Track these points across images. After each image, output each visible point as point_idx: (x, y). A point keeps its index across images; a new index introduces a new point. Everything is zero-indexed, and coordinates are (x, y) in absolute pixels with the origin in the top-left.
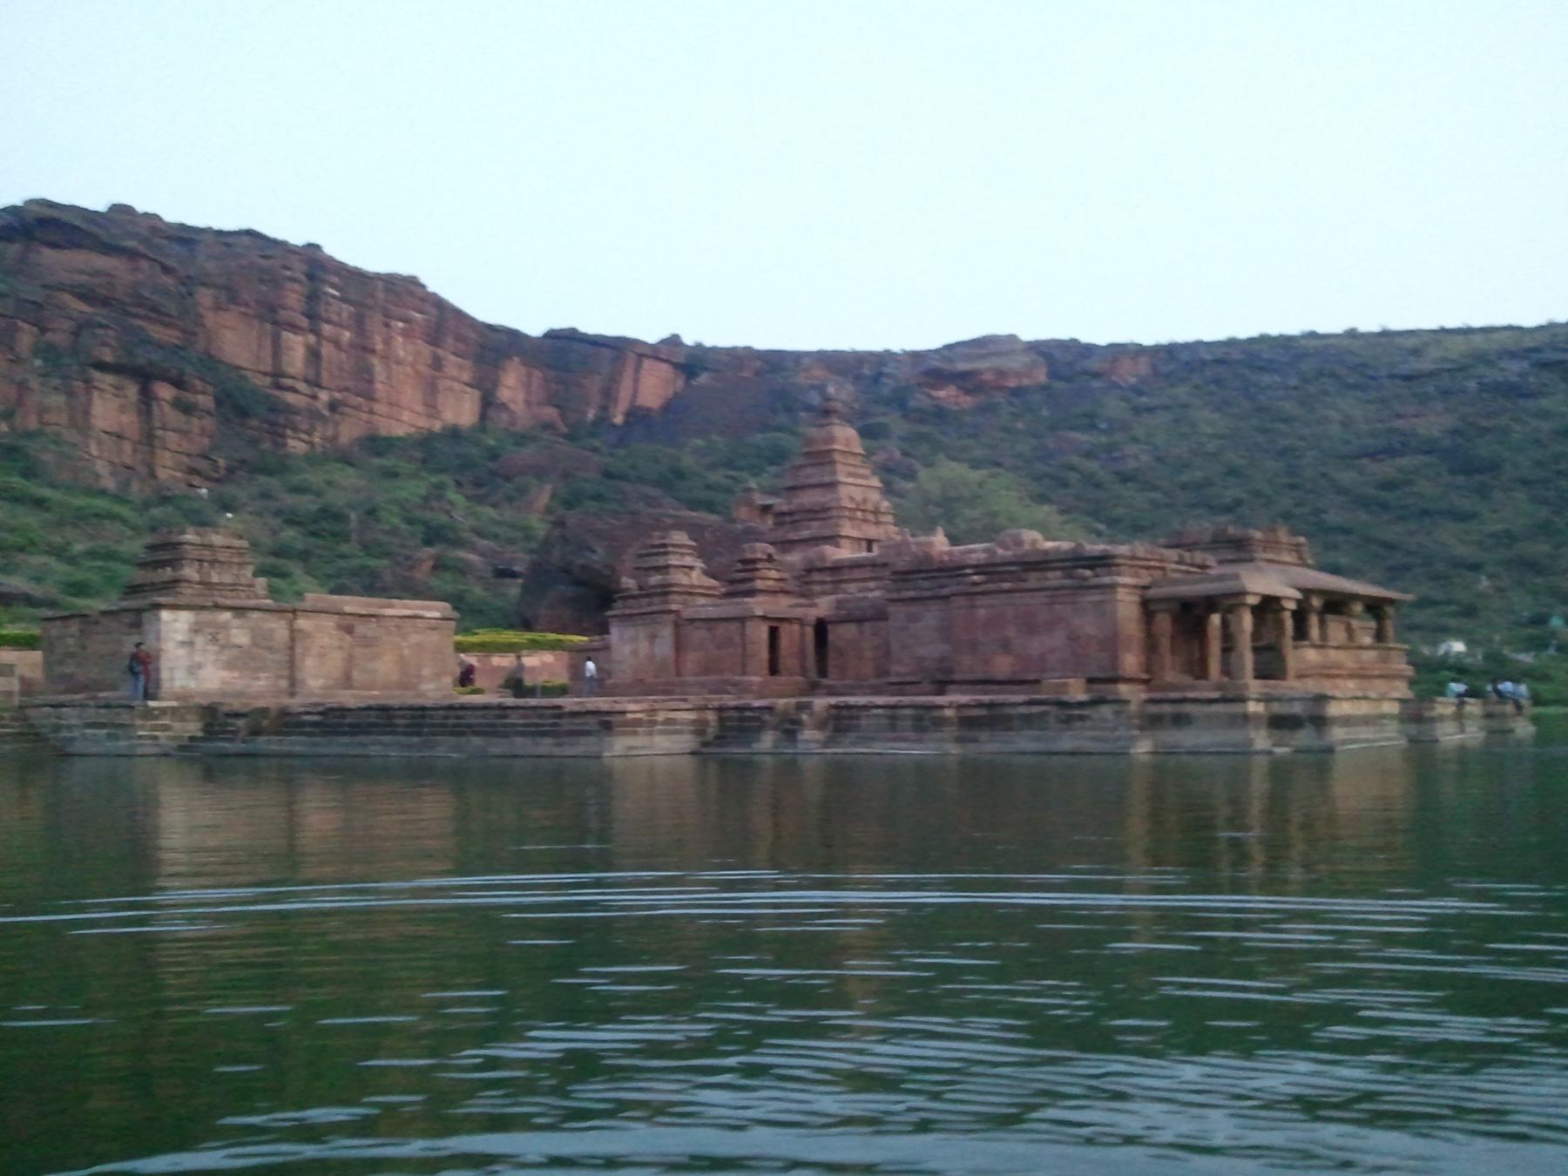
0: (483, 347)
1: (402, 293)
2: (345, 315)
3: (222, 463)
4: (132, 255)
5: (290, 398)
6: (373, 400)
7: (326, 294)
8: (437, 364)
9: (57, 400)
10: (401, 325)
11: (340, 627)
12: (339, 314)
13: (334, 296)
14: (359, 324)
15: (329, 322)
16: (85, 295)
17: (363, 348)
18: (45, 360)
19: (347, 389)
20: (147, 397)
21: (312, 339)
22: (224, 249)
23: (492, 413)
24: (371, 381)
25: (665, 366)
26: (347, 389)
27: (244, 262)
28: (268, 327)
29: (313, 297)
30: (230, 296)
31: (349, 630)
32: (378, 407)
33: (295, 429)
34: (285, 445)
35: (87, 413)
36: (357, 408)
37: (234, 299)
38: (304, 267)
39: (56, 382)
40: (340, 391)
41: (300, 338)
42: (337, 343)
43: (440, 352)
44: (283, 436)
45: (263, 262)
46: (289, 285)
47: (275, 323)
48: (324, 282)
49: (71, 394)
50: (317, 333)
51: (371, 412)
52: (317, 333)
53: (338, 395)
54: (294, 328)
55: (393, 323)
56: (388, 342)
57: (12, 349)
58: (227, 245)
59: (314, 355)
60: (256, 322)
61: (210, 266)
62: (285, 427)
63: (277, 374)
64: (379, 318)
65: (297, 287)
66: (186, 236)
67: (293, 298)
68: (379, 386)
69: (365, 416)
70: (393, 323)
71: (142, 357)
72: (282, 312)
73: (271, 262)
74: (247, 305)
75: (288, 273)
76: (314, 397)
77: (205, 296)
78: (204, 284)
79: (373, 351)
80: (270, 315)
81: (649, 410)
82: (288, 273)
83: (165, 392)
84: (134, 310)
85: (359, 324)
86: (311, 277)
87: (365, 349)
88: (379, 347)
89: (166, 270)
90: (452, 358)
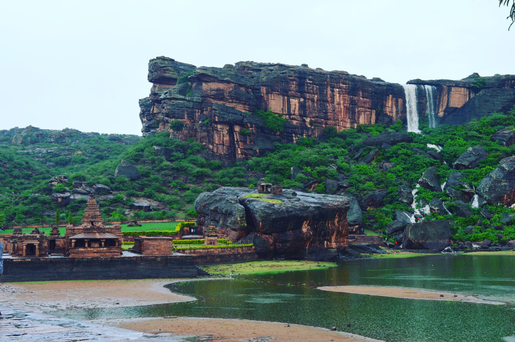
0: (375, 93)
1: (338, 78)
2: (315, 89)
3: (258, 151)
4: (228, 82)
5: (295, 122)
6: (328, 120)
7: (307, 83)
8: (353, 103)
9: (205, 134)
10: (338, 90)
11: (4, 240)
12: (313, 90)
13: (310, 83)
14: (321, 92)
15: (308, 93)
16: (215, 97)
17: (323, 101)
18: (203, 121)
19: (316, 117)
20: (231, 132)
21: (302, 100)
22: (270, 72)
23: (381, 118)
24: (326, 113)
25: (463, 89)
26: (316, 117)
27: (275, 76)
28: (286, 97)
29: (301, 85)
30: (271, 90)
31: (7, 240)
32: (329, 122)
33: (296, 134)
34: (293, 140)
35: (213, 136)
36: (321, 123)
37: (273, 90)
38: (297, 75)
39: (204, 128)
40: (313, 118)
41: (297, 101)
42: (313, 100)
43: (355, 98)
44: (292, 137)
45: (282, 75)
46: (291, 82)
47: (288, 96)
48: (305, 79)
49: (208, 132)
50: (305, 98)
51: (326, 124)
52: (305, 98)
53: (313, 119)
54: (294, 97)
55: (335, 89)
56: (333, 97)
57: (193, 119)
58: (271, 70)
59: (302, 106)
60: (282, 97)
61: (264, 79)
62: (292, 133)
63: (290, 114)
64: (329, 88)
65: (294, 82)
66: (259, 68)
67: (293, 86)
68: (329, 114)
69: (324, 126)
70: (335, 89)
71: (230, 117)
72: (290, 92)
73: (284, 75)
74: (278, 91)
75: (291, 78)
76: (304, 121)
77: (264, 90)
78: (263, 86)
79: (327, 102)
80: (285, 93)
81: (456, 108)
82: (291, 78)
83: (237, 129)
84: (231, 101)
85: (321, 92)
86: (299, 78)
87: (324, 101)
88: (329, 99)
89: (241, 85)
90: (361, 98)
